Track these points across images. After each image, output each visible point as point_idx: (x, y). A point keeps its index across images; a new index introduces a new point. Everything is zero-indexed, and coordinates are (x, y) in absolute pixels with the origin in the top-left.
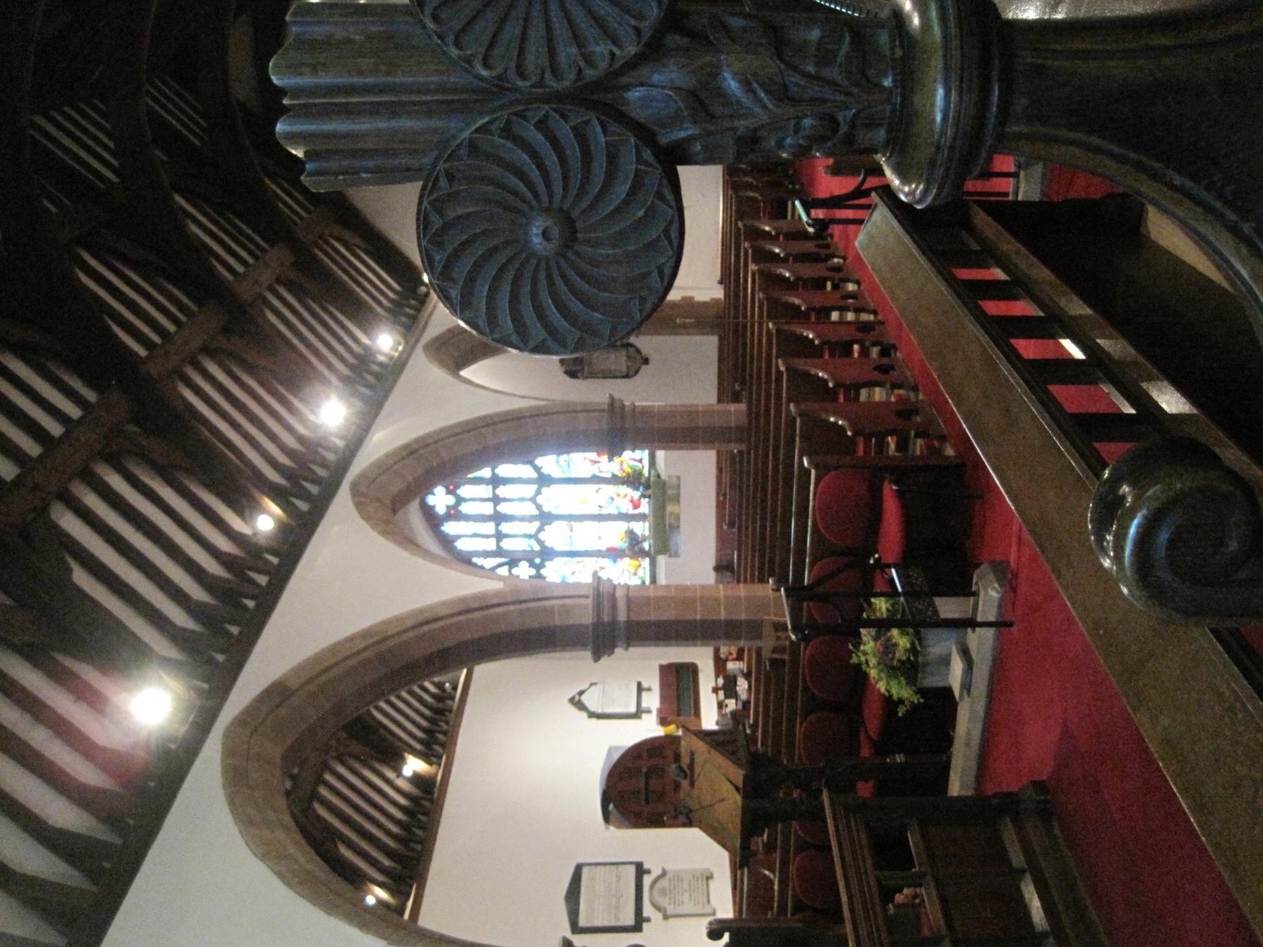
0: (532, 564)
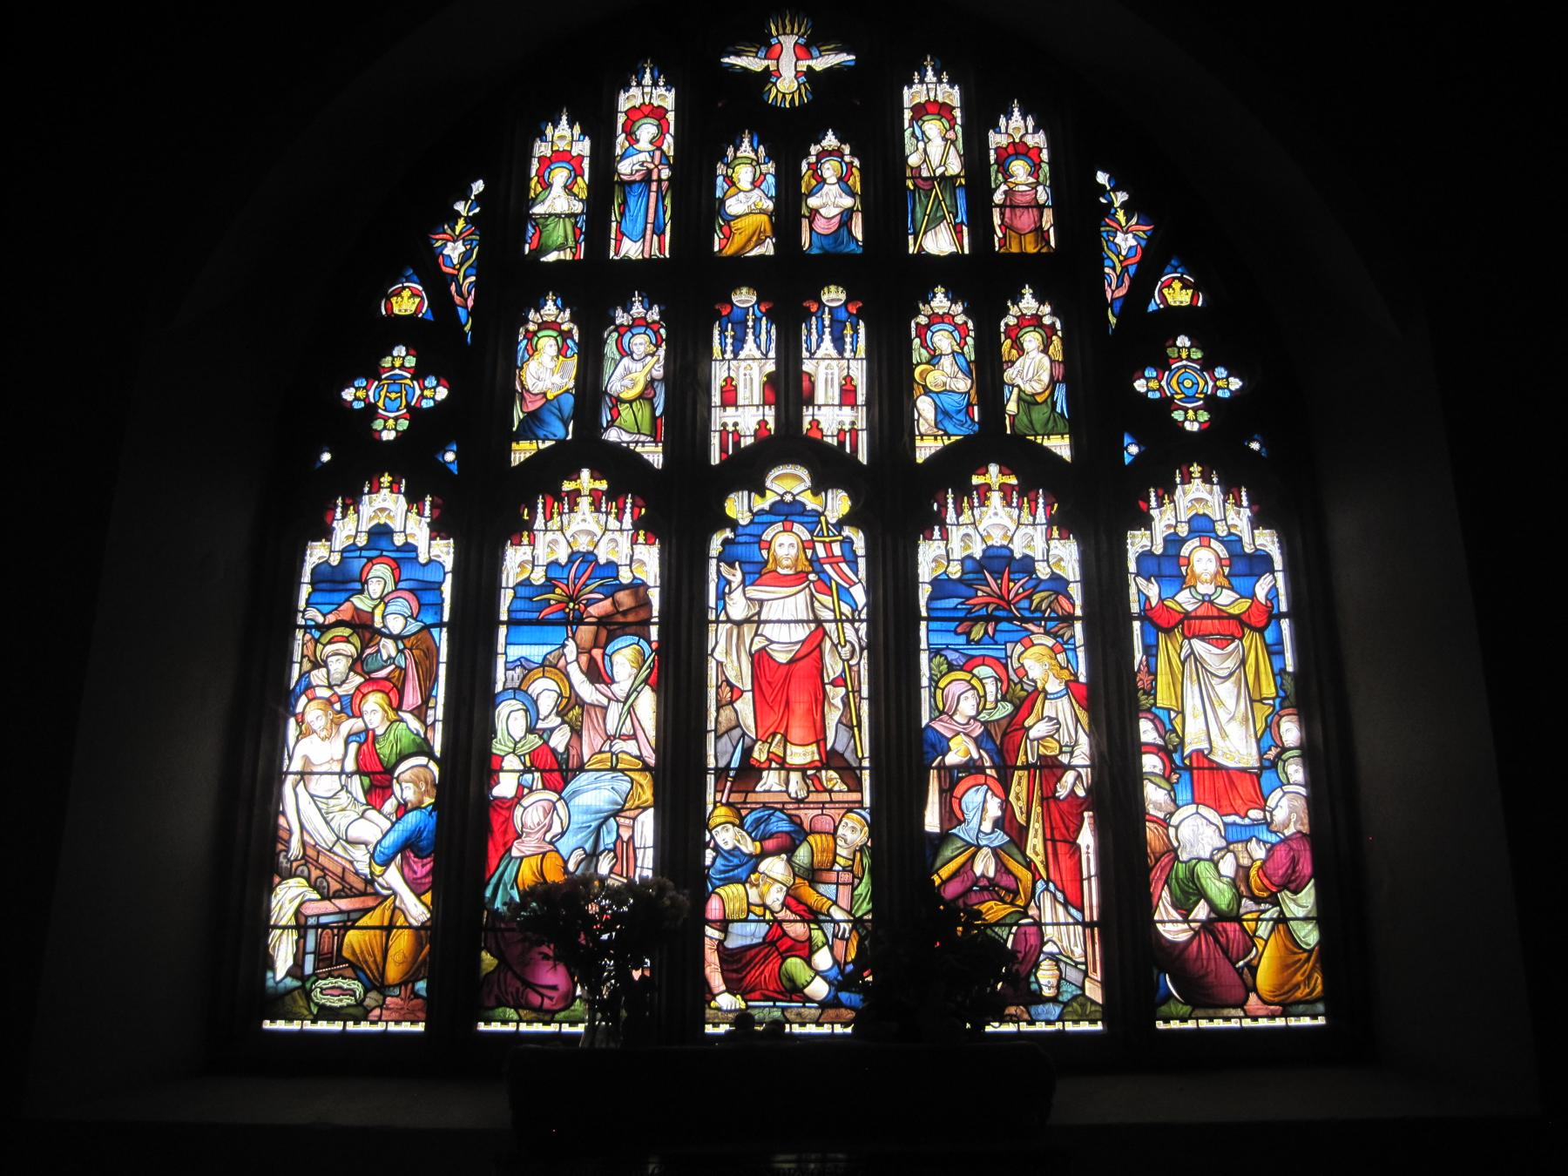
0: (427, 427)
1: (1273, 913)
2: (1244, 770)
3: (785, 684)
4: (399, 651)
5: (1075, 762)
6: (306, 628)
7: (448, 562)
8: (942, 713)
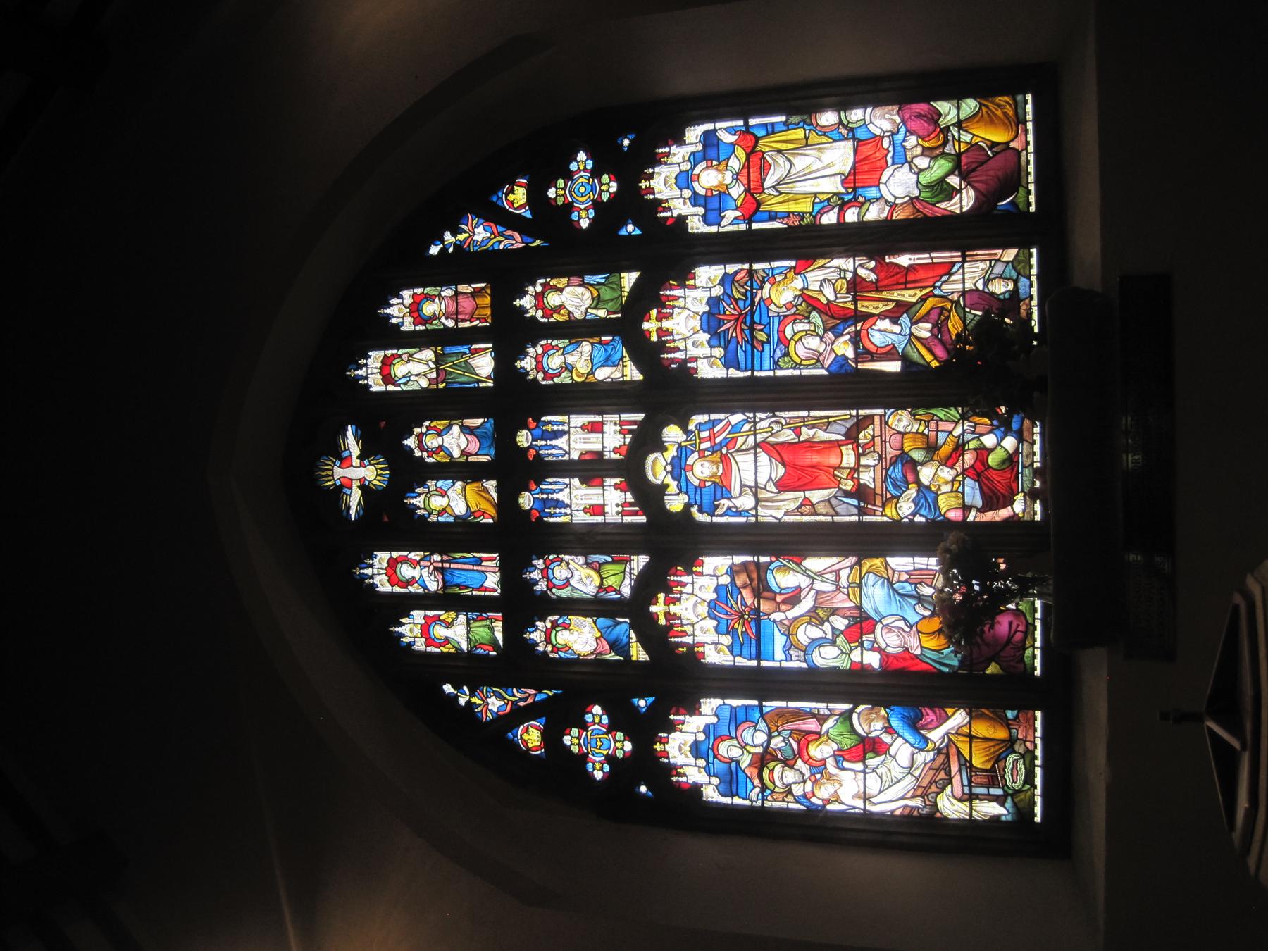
0: (621, 720)
1: (954, 131)
2: (856, 151)
3: (799, 470)
4: (779, 734)
5: (851, 269)
6: (763, 800)
7: (717, 702)
8: (818, 360)
